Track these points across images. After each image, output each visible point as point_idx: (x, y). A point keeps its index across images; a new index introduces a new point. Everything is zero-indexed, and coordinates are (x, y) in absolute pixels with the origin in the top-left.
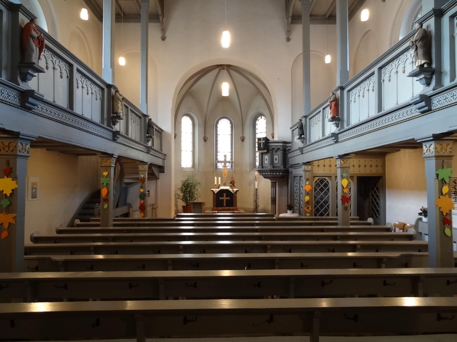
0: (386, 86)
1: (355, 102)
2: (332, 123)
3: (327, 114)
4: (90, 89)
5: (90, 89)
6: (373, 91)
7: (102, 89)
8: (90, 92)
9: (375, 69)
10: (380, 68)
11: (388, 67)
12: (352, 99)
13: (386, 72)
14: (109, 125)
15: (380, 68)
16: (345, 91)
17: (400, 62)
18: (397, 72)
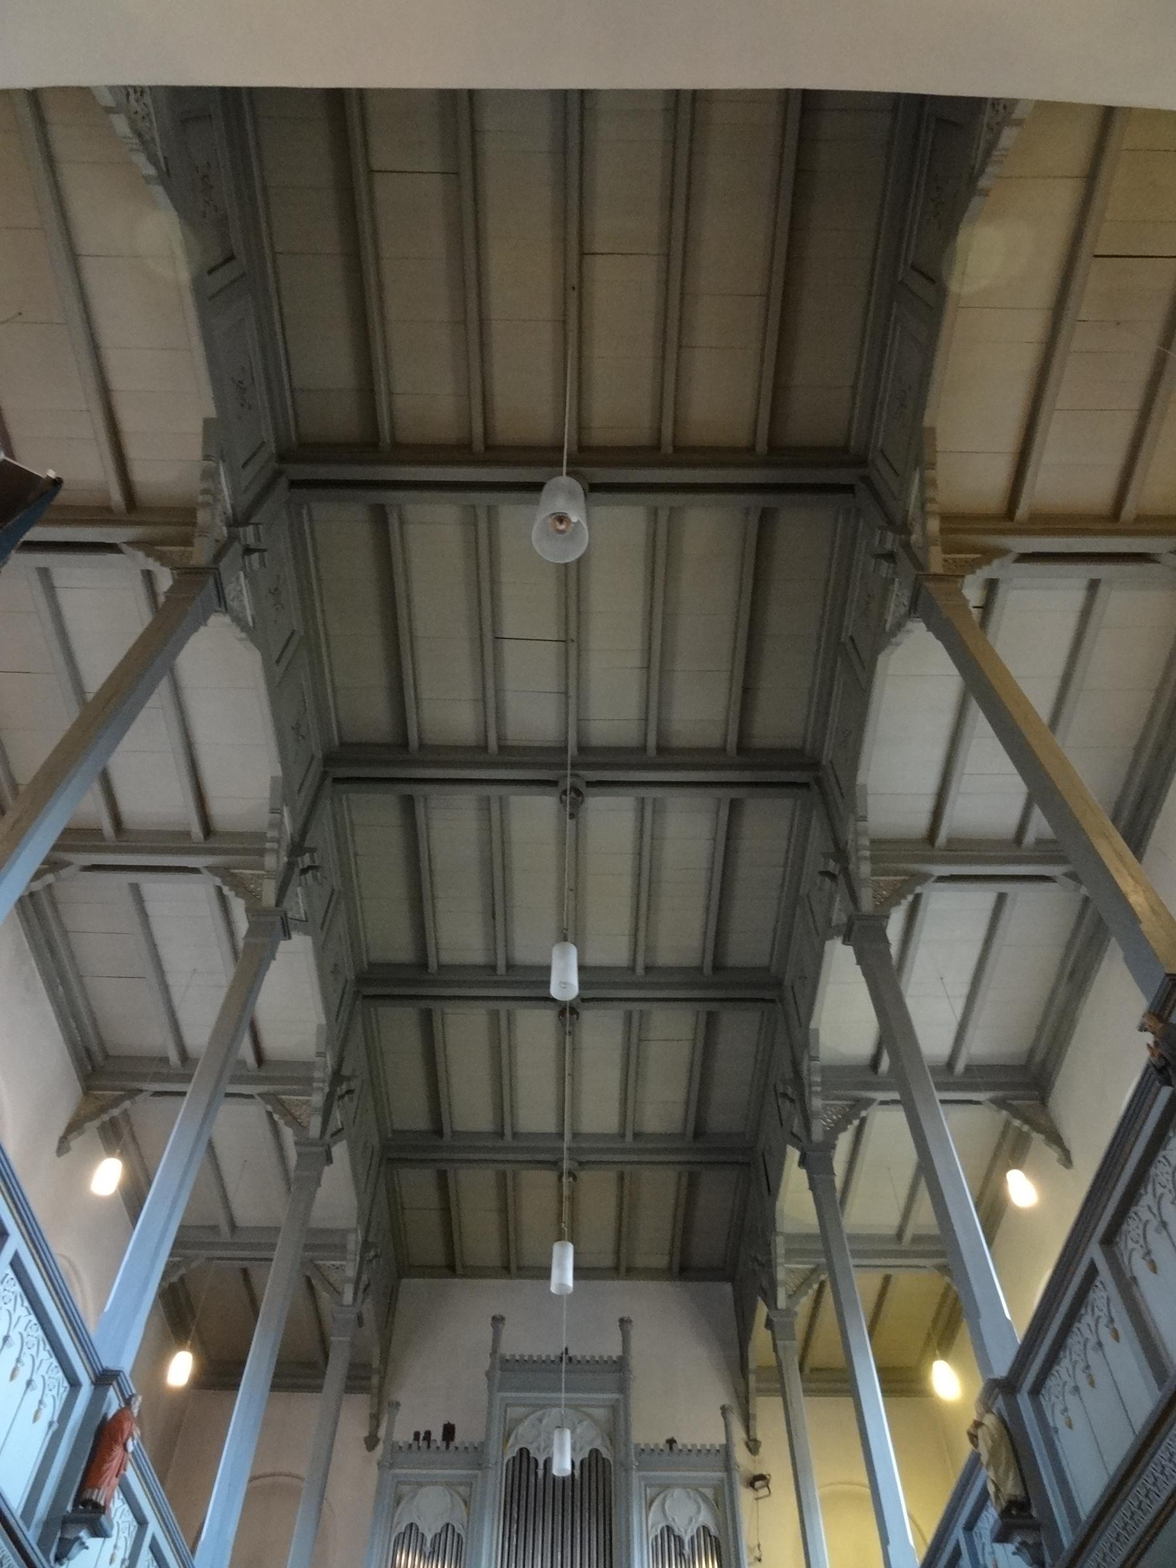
0: (1149, 1287)
1: (1070, 1426)
2: (1010, 1547)
3: (988, 1549)
4: (27, 1360)
5: (27, 1360)
6: (1116, 1337)
7: (74, 1384)
8: (24, 1374)
9: (1094, 1251)
10: (1109, 1240)
11: (1132, 1227)
12: (1056, 1420)
13: (1131, 1245)
14: (43, 1543)
15: (1109, 1240)
16: (1024, 1400)
17: (1159, 1190)
18: (1164, 1225)
